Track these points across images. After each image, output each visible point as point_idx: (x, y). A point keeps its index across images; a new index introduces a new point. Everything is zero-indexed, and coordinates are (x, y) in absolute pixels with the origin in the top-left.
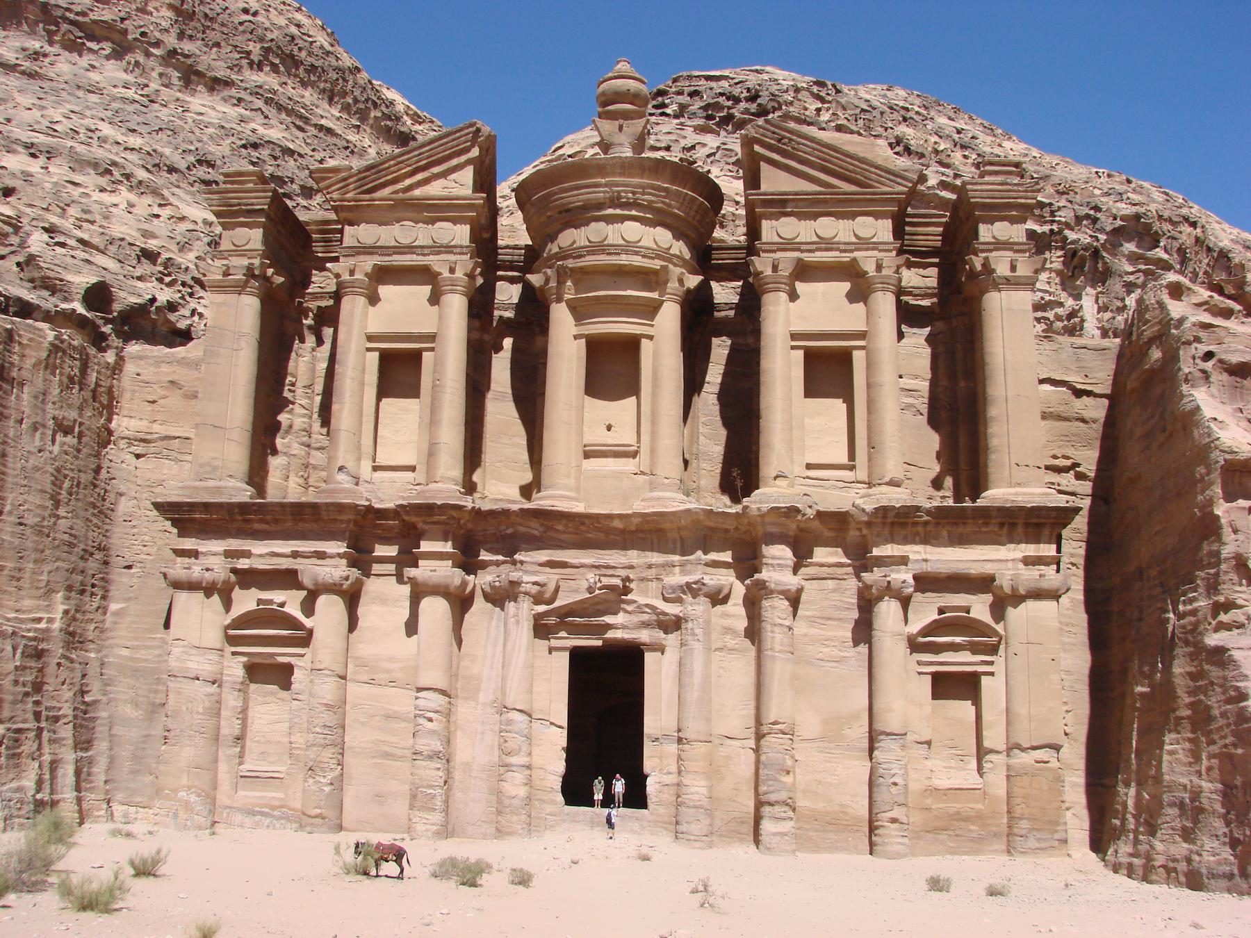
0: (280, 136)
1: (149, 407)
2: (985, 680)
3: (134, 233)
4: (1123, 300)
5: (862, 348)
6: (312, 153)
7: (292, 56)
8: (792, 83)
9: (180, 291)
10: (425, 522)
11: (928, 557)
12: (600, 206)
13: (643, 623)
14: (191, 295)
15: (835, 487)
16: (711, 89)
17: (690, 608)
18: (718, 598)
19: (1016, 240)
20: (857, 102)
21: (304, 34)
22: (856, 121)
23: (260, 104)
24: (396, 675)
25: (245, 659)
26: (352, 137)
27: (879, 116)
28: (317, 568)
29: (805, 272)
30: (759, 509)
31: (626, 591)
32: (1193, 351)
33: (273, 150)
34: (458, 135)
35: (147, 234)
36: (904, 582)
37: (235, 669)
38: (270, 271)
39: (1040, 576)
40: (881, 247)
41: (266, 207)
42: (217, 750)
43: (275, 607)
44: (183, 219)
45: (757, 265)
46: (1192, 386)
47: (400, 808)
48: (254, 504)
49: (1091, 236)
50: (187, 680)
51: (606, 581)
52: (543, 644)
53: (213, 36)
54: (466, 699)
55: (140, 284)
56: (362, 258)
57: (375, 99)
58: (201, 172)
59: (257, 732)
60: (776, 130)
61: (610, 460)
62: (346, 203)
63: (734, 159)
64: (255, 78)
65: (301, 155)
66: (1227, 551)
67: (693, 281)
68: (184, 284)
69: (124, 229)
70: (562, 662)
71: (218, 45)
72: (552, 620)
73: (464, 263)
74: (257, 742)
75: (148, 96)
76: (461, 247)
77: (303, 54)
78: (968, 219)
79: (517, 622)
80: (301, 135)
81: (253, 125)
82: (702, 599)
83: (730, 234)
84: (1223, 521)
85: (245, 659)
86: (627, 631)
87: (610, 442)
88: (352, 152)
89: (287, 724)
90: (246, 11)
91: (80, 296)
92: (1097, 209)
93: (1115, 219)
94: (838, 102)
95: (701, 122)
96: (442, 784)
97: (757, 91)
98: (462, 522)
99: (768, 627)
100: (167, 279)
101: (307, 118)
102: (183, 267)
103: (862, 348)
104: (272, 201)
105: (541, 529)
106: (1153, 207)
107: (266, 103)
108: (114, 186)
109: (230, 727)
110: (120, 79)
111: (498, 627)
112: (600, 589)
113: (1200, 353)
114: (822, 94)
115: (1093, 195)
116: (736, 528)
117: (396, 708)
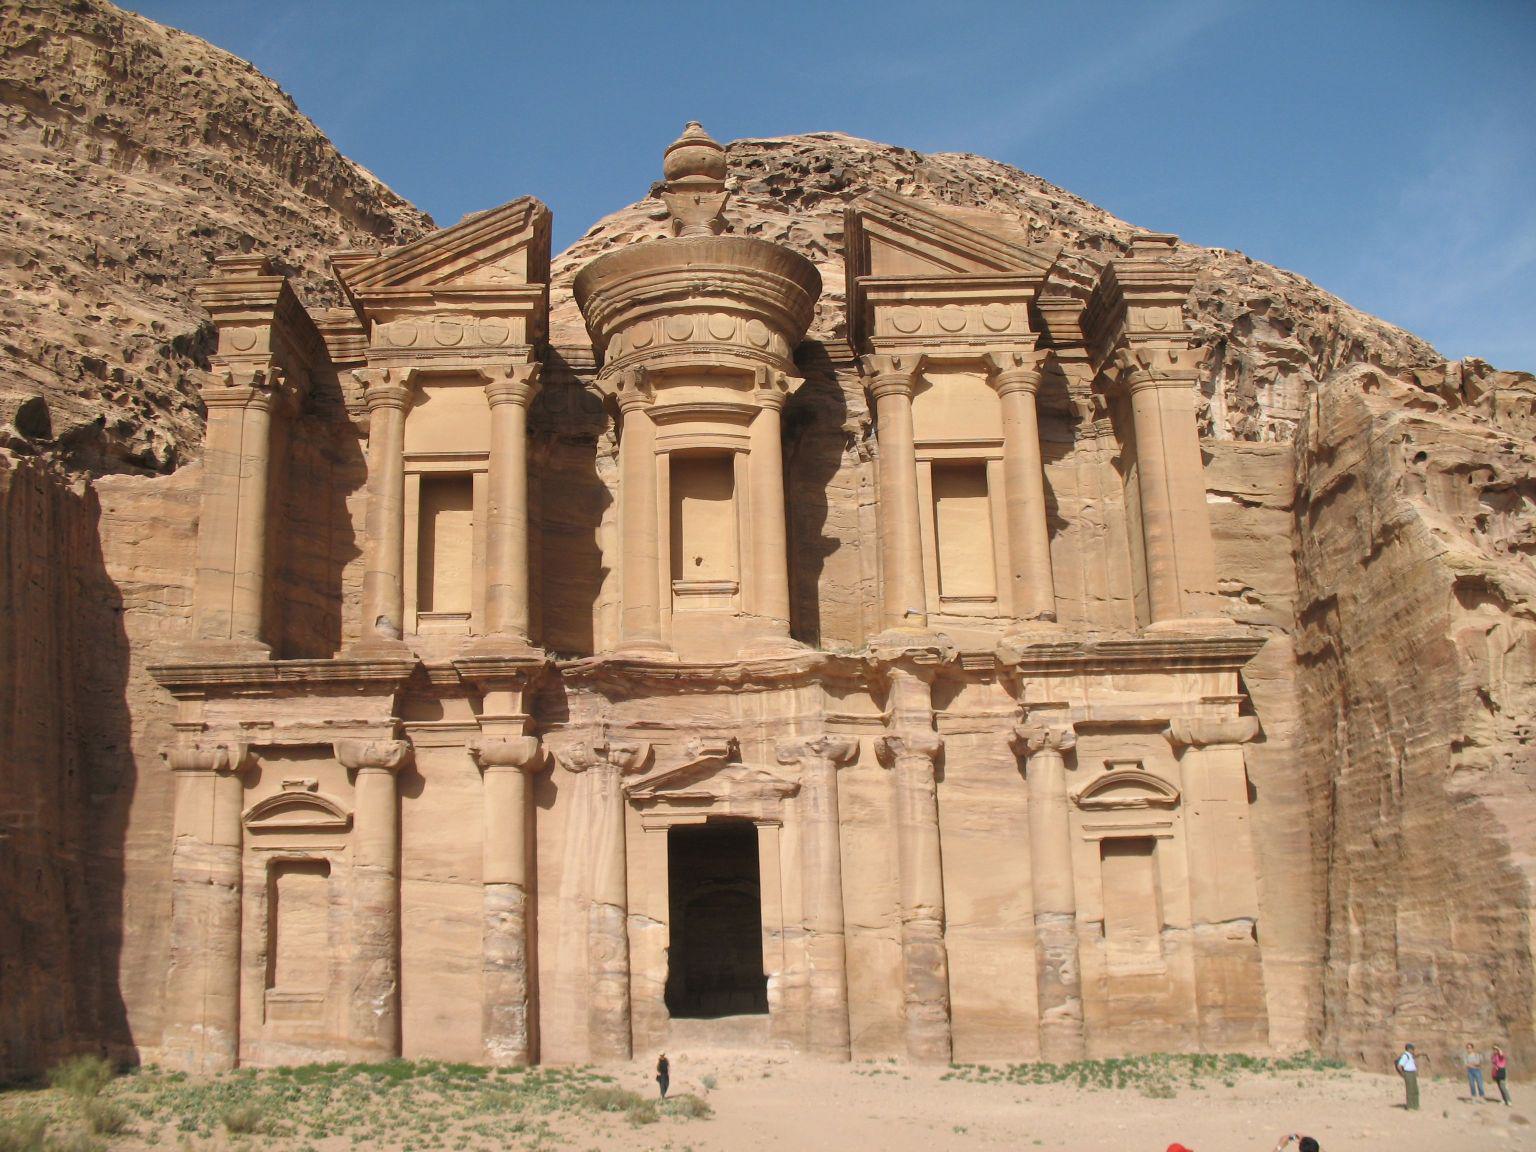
0: (236, 221)
1: (128, 550)
2: (1161, 845)
3: (70, 340)
4: (1254, 398)
5: (1001, 459)
6: (274, 242)
7: (246, 125)
8: (866, 151)
9: (132, 409)
11: (1091, 703)
12: (682, 295)
14: (148, 414)
15: (975, 625)
16: (773, 159)
17: (811, 774)
18: (844, 759)
19: (1172, 329)
20: (941, 173)
21: (258, 98)
22: (942, 194)
23: (209, 182)
26: (322, 222)
27: (967, 189)
28: (355, 741)
29: (928, 365)
30: (891, 653)
31: (733, 756)
32: (1403, 451)
33: (229, 237)
34: (508, 212)
35: (84, 341)
36: (1065, 733)
37: (256, 872)
38: (282, 380)
39: (1223, 720)
40: (1017, 339)
41: (274, 302)
42: (238, 973)
44: (128, 321)
45: (873, 363)
46: (1406, 493)
47: (472, 1030)
48: (276, 666)
49: (1216, 325)
50: (197, 885)
53: (152, 100)
55: (84, 402)
56: (395, 362)
57: (345, 175)
58: (142, 265)
60: (889, 204)
61: (705, 600)
63: (807, 242)
64: (202, 151)
65: (263, 245)
66: (1467, 682)
67: (795, 384)
68: (136, 401)
69: (58, 334)
70: (660, 845)
71: (156, 111)
72: (646, 793)
73: (524, 368)
75: (73, 173)
76: (517, 347)
77: (259, 122)
78: (1113, 305)
79: (605, 798)
80: (261, 220)
81: (202, 208)
83: (825, 327)
84: (1458, 647)
85: (268, 855)
87: (700, 578)
88: (322, 240)
89: (324, 935)
90: (187, 70)
91: (12, 417)
92: (1219, 292)
93: (1242, 304)
94: (921, 173)
95: (767, 198)
96: (522, 1000)
97: (828, 160)
98: (533, 679)
99: (907, 793)
100: (116, 395)
101: (268, 200)
102: (135, 379)
103: (1001, 459)
104: (282, 295)
105: (628, 685)
106: (1281, 290)
107: (217, 181)
108: (42, 282)
109: (254, 940)
110: (38, 152)
113: (1411, 455)
114: (902, 163)
115: (1213, 278)
116: (861, 678)
117: (459, 909)
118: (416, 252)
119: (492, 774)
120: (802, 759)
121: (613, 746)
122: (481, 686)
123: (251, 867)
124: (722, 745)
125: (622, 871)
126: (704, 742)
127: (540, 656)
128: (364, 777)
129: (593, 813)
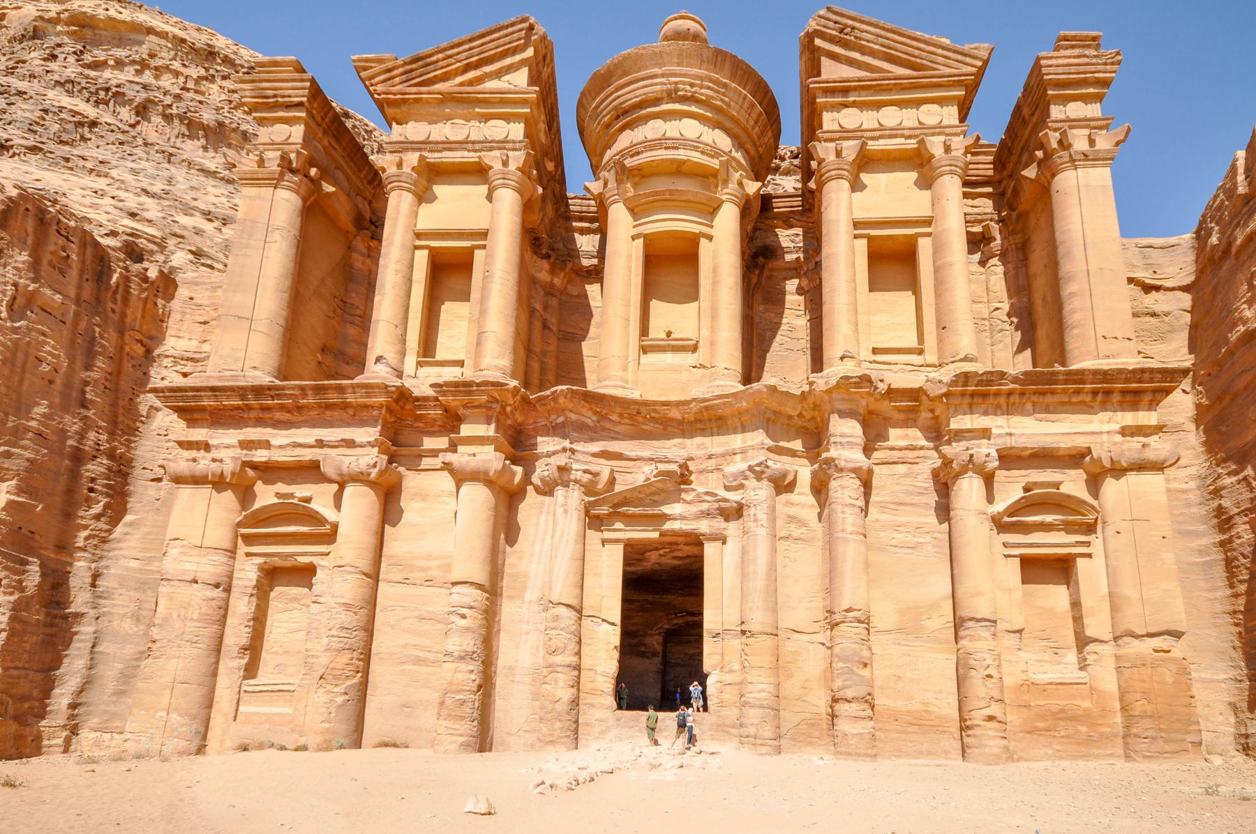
10: (465, 406)
13: (703, 512)
17: (753, 493)
18: (783, 485)
24: (435, 573)
25: (260, 560)
37: (248, 573)
43: (295, 501)
51: (662, 467)
52: (594, 536)
54: (511, 598)
59: (275, 642)
62: (391, 96)
72: (604, 510)
74: (273, 653)
79: (566, 511)
82: (765, 483)
85: (260, 560)
86: (684, 522)
89: (304, 633)
111: (547, 520)
112: (655, 476)
117: (431, 609)
118: (429, 60)
119: (466, 489)
120: (745, 482)
121: (575, 466)
122: (461, 411)
123: (243, 570)
124: (674, 467)
125: (579, 576)
126: (658, 465)
127: (514, 383)
128: (349, 490)
129: (555, 523)
